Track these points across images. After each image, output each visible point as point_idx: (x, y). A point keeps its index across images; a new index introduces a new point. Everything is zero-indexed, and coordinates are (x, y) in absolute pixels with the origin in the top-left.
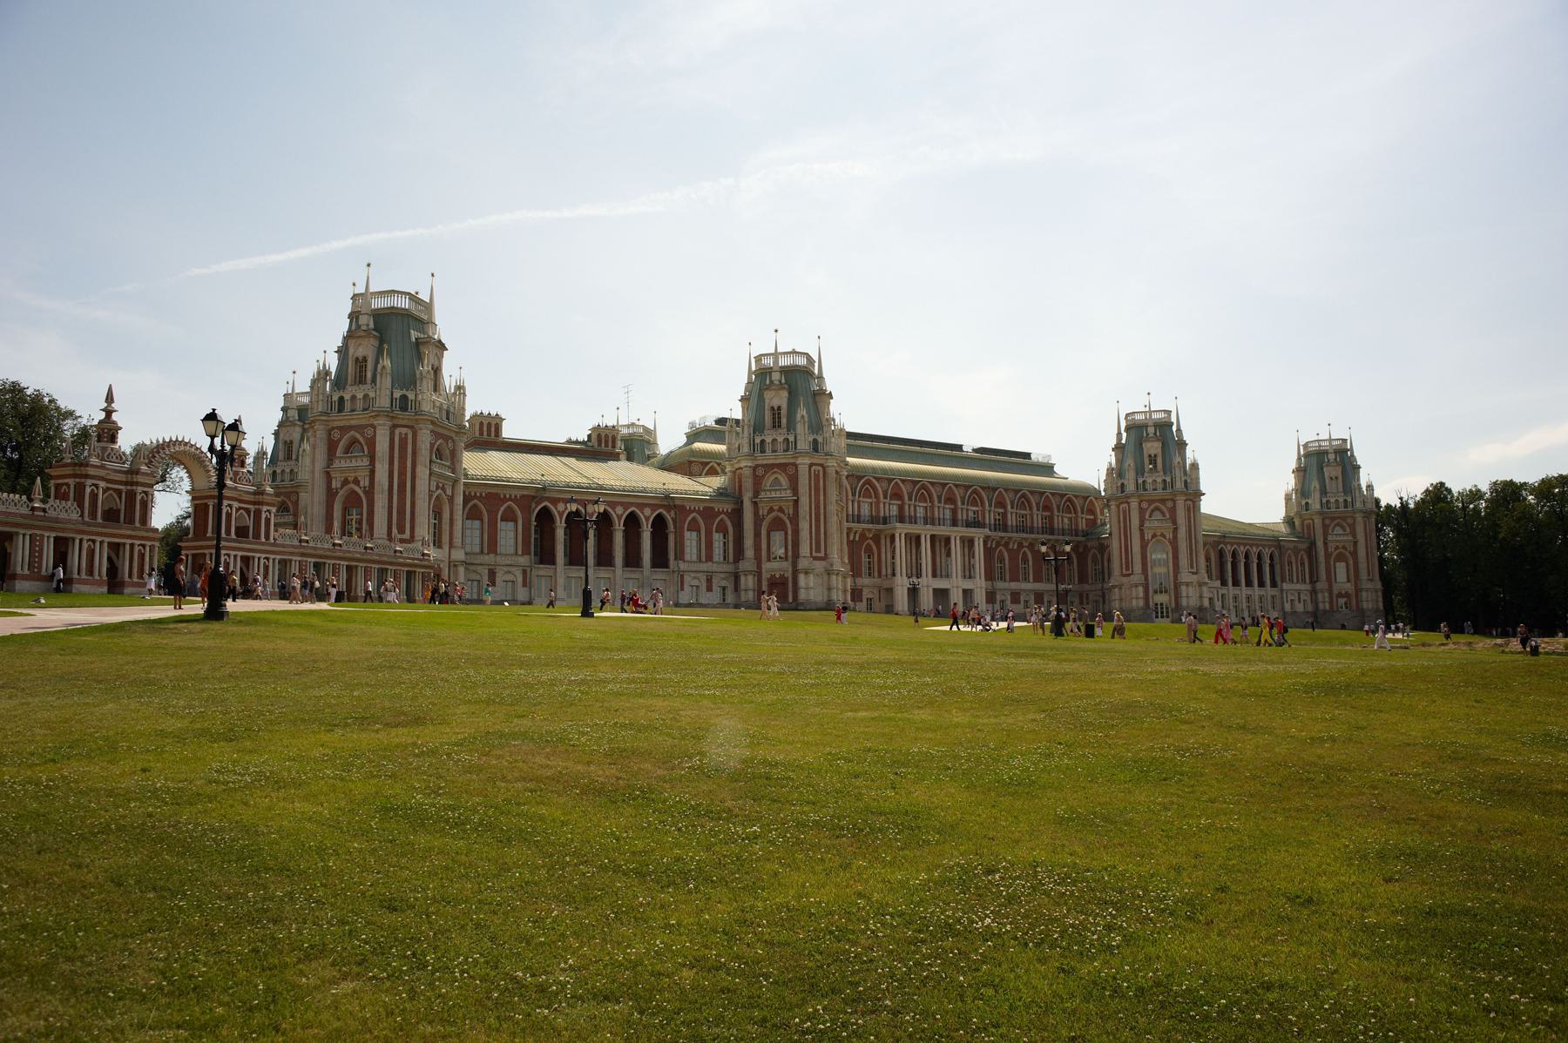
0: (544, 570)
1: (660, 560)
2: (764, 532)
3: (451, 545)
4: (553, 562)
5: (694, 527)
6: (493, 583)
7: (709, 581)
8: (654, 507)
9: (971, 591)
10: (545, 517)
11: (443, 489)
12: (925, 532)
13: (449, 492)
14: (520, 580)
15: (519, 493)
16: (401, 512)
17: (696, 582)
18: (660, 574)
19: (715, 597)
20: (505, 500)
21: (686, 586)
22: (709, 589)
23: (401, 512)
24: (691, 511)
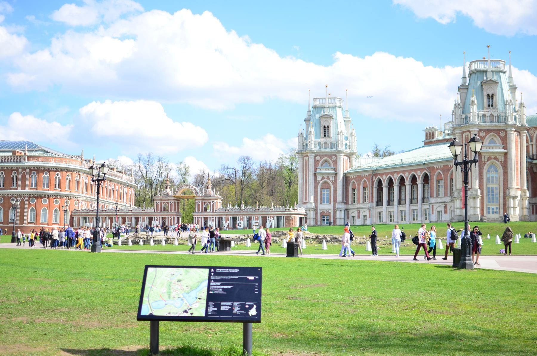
0: (379, 209)
3: (335, 201)
4: (382, 205)
6: (359, 217)
8: (422, 170)
10: (380, 183)
11: (328, 178)
13: (332, 178)
15: (367, 174)
16: (306, 192)
17: (439, 209)
18: (426, 207)
21: (434, 212)
22: (446, 212)
23: (306, 192)
24: (437, 169)
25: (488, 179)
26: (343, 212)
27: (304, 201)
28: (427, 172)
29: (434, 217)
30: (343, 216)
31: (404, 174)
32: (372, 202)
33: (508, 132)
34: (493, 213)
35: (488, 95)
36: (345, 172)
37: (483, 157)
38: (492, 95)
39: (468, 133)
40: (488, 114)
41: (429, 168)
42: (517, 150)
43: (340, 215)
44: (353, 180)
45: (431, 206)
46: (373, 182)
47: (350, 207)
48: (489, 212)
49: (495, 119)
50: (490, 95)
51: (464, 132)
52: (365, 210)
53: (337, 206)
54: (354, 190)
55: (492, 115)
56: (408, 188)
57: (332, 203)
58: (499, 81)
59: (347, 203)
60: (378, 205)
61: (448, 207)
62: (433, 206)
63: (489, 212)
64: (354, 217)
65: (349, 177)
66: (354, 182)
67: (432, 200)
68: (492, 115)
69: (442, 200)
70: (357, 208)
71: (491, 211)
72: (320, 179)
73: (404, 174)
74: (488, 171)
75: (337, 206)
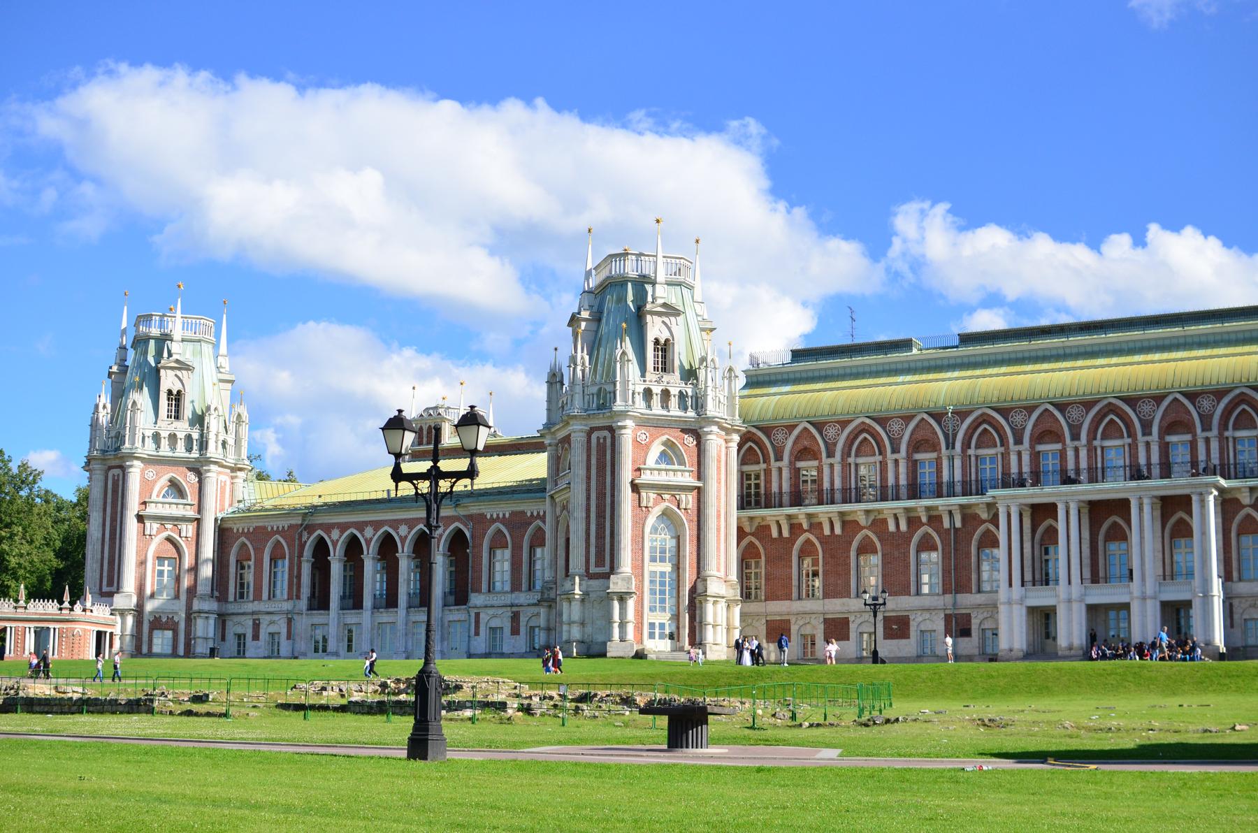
0: (318, 617)
1: (459, 594)
2: (561, 542)
5: (498, 542)
6: (256, 637)
7: (515, 618)
9: (1188, 604)
10: (321, 549)
12: (1069, 499)
13: (189, 530)
14: (284, 631)
15: (285, 523)
16: (111, 562)
19: (521, 643)
20: (273, 533)
21: (482, 629)
22: (515, 631)
24: (493, 521)
25: (653, 549)
26: (212, 622)
27: (105, 589)
28: (462, 527)
29: (480, 644)
30: (211, 634)
31: (396, 529)
32: (298, 597)
33: (703, 439)
34: (662, 636)
35: (657, 342)
36: (220, 516)
37: (643, 494)
38: (667, 341)
39: (606, 433)
40: (657, 390)
41: (470, 517)
42: (719, 482)
43: (205, 628)
44: (243, 539)
45: (473, 615)
46: (302, 546)
47: (232, 608)
48: (652, 636)
49: (674, 402)
50: (662, 341)
51: (593, 430)
52: (275, 618)
53: (196, 605)
54: (241, 566)
55: (666, 394)
56: (405, 565)
57: (183, 597)
58: (681, 308)
59: (222, 598)
60: (310, 608)
61: (523, 620)
62: (477, 615)
63: (652, 636)
64: (240, 637)
65: (231, 529)
66: (244, 545)
67: (476, 599)
68: (666, 394)
69: (508, 599)
70: (253, 613)
71: (657, 631)
72: (154, 532)
73: (396, 529)
74: (655, 530)
75: (196, 605)
